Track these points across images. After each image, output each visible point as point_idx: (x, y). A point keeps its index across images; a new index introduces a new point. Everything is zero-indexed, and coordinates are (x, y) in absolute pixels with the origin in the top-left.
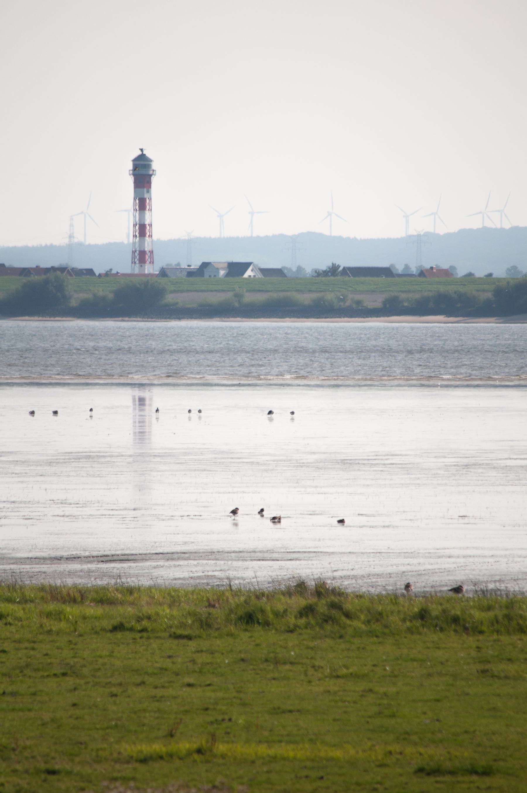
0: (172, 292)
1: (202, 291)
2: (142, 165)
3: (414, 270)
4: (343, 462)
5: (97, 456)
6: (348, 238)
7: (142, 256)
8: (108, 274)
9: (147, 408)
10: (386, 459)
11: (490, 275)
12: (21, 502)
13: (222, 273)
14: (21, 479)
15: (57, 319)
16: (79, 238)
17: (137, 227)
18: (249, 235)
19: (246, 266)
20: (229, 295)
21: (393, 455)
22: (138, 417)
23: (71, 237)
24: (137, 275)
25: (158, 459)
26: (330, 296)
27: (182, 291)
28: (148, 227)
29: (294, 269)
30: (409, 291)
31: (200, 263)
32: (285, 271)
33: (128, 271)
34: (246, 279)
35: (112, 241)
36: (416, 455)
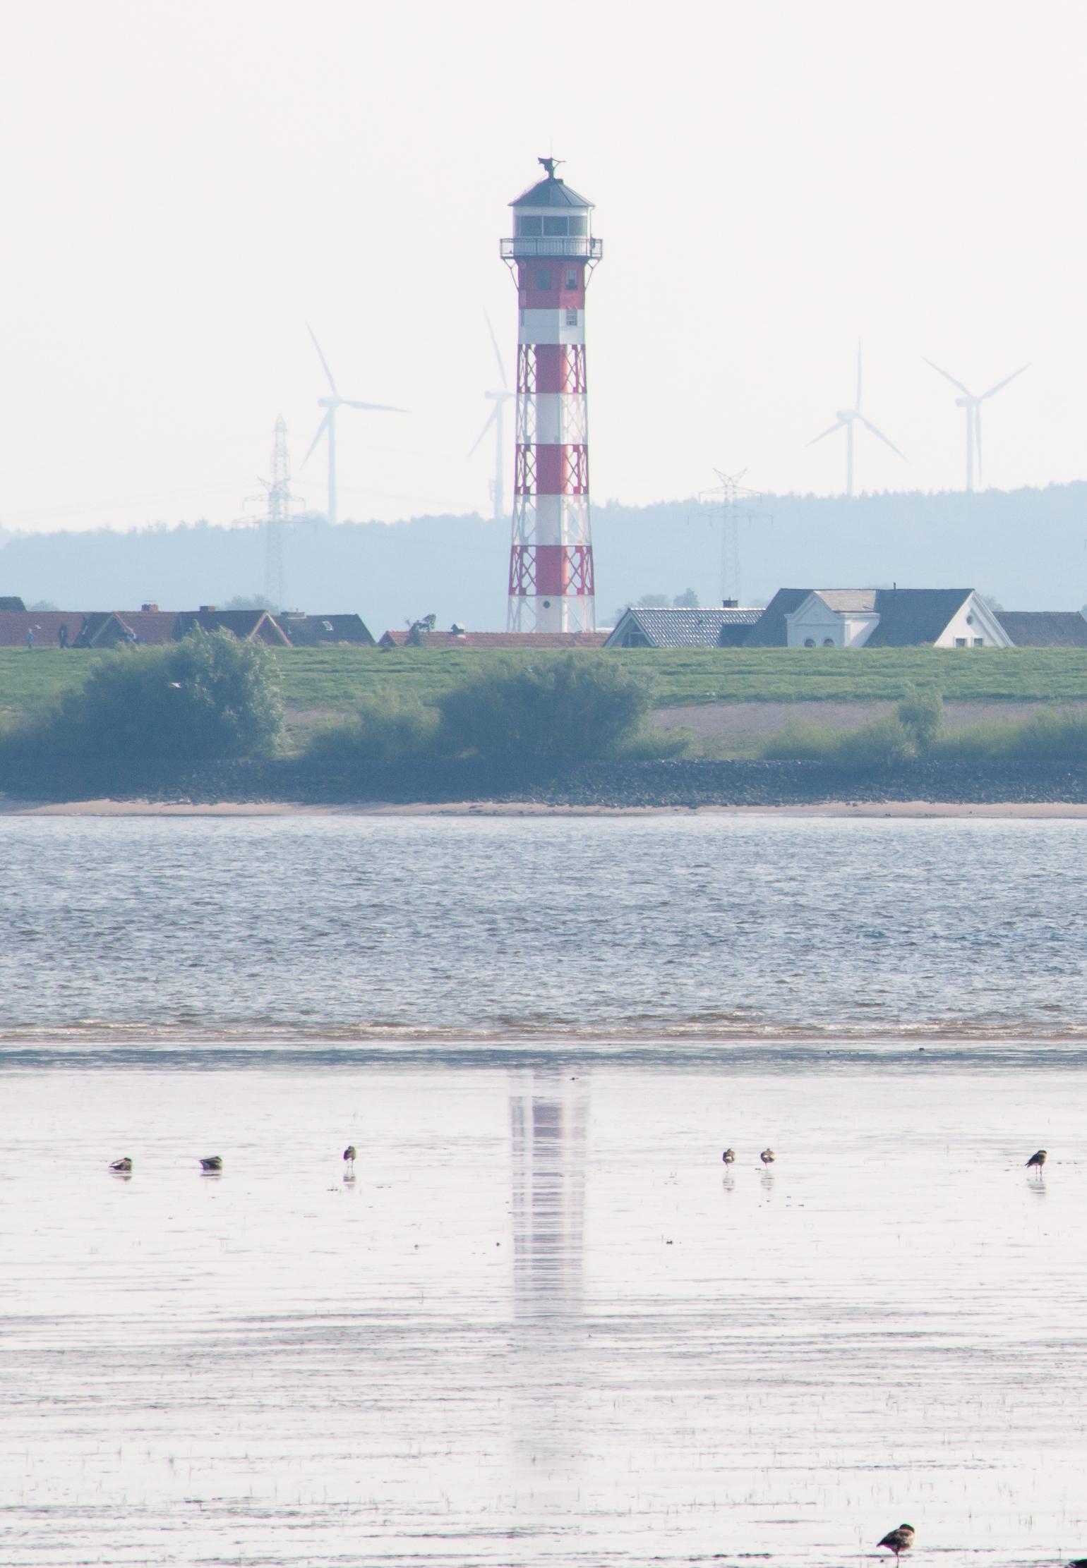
0: (663, 702)
1: (779, 699)
2: (549, 219)
5: (371, 1329)
7: (548, 569)
8: (414, 636)
9: (566, 1143)
12: (72, 1512)
13: (855, 629)
14: (75, 1422)
15: (223, 807)
16: (308, 499)
17: (531, 458)
18: (960, 486)
19: (943, 604)
20: (883, 715)
22: (530, 1180)
23: (277, 494)
24: (530, 639)
25: (607, 1341)
27: (702, 700)
28: (572, 458)
31: (769, 595)
33: (497, 624)
34: (946, 652)
35: (436, 511)
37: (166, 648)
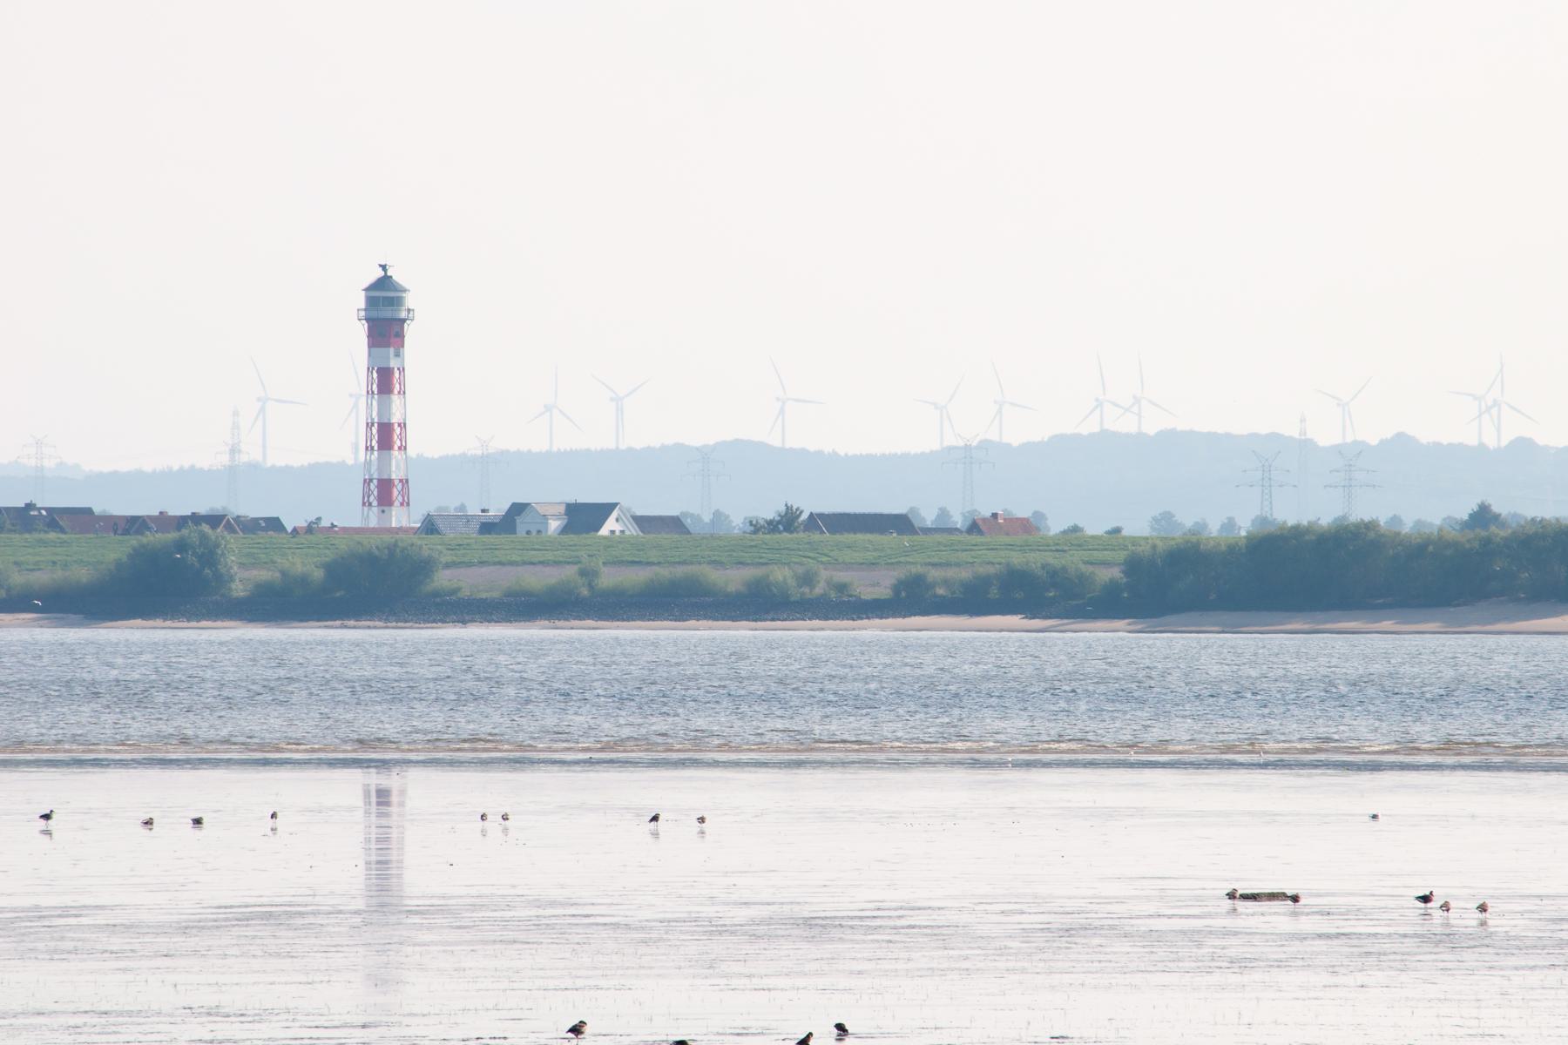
0: (447, 566)
1: (512, 563)
2: (385, 298)
3: (958, 521)
4: (809, 922)
5: (286, 913)
6: (820, 453)
7: (384, 492)
8: (310, 529)
9: (394, 809)
10: (900, 917)
11: (1117, 531)
12: (120, 1014)
13: (554, 525)
14: (122, 964)
15: (204, 623)
16: (251, 453)
17: (375, 430)
18: (612, 446)
19: (605, 510)
20: (570, 572)
21: (913, 909)
22: (374, 830)
23: (234, 450)
24: (373, 531)
25: (416, 919)
26: (781, 575)
27: (469, 565)
28: (398, 430)
29: (707, 518)
30: (948, 565)
31: (506, 506)
32: (688, 522)
33: (356, 523)
34: (605, 538)
35: (322, 460)
36: (961, 909)
37: (172, 536)
